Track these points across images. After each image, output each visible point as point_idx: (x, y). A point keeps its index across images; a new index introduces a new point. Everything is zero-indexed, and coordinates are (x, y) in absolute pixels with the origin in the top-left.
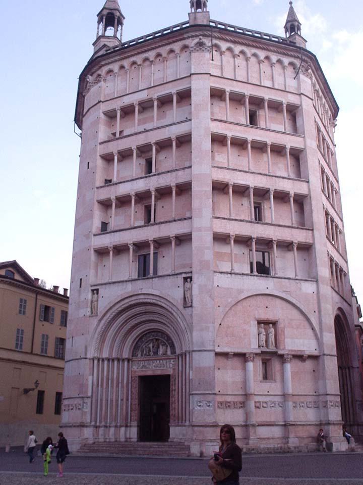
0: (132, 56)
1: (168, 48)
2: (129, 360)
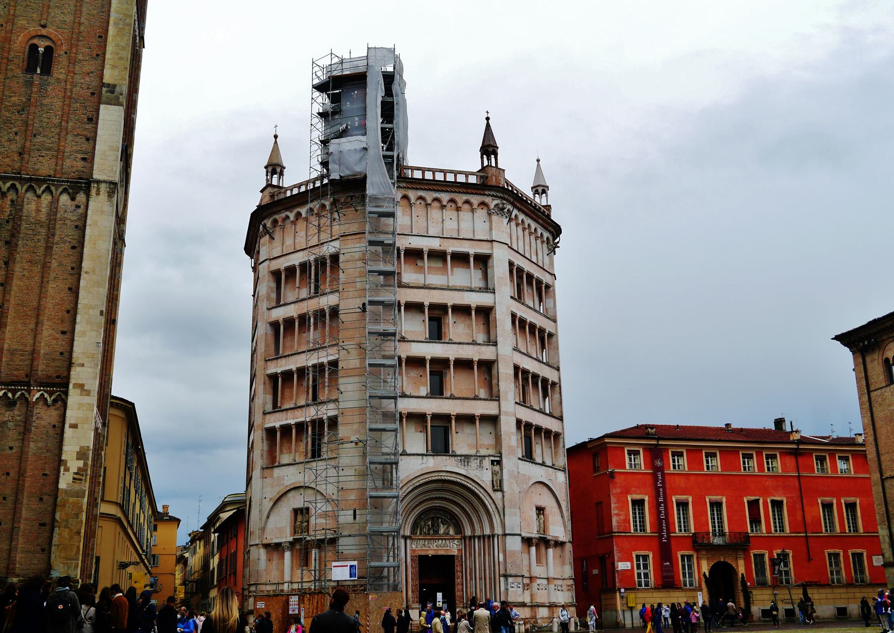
0: (421, 189)
1: (465, 197)
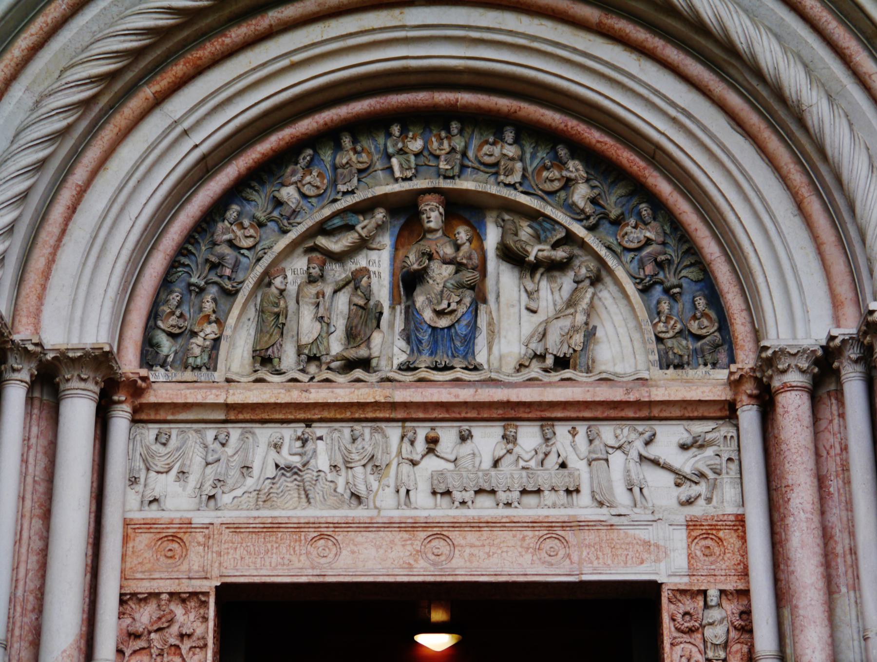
2: (110, 392)
